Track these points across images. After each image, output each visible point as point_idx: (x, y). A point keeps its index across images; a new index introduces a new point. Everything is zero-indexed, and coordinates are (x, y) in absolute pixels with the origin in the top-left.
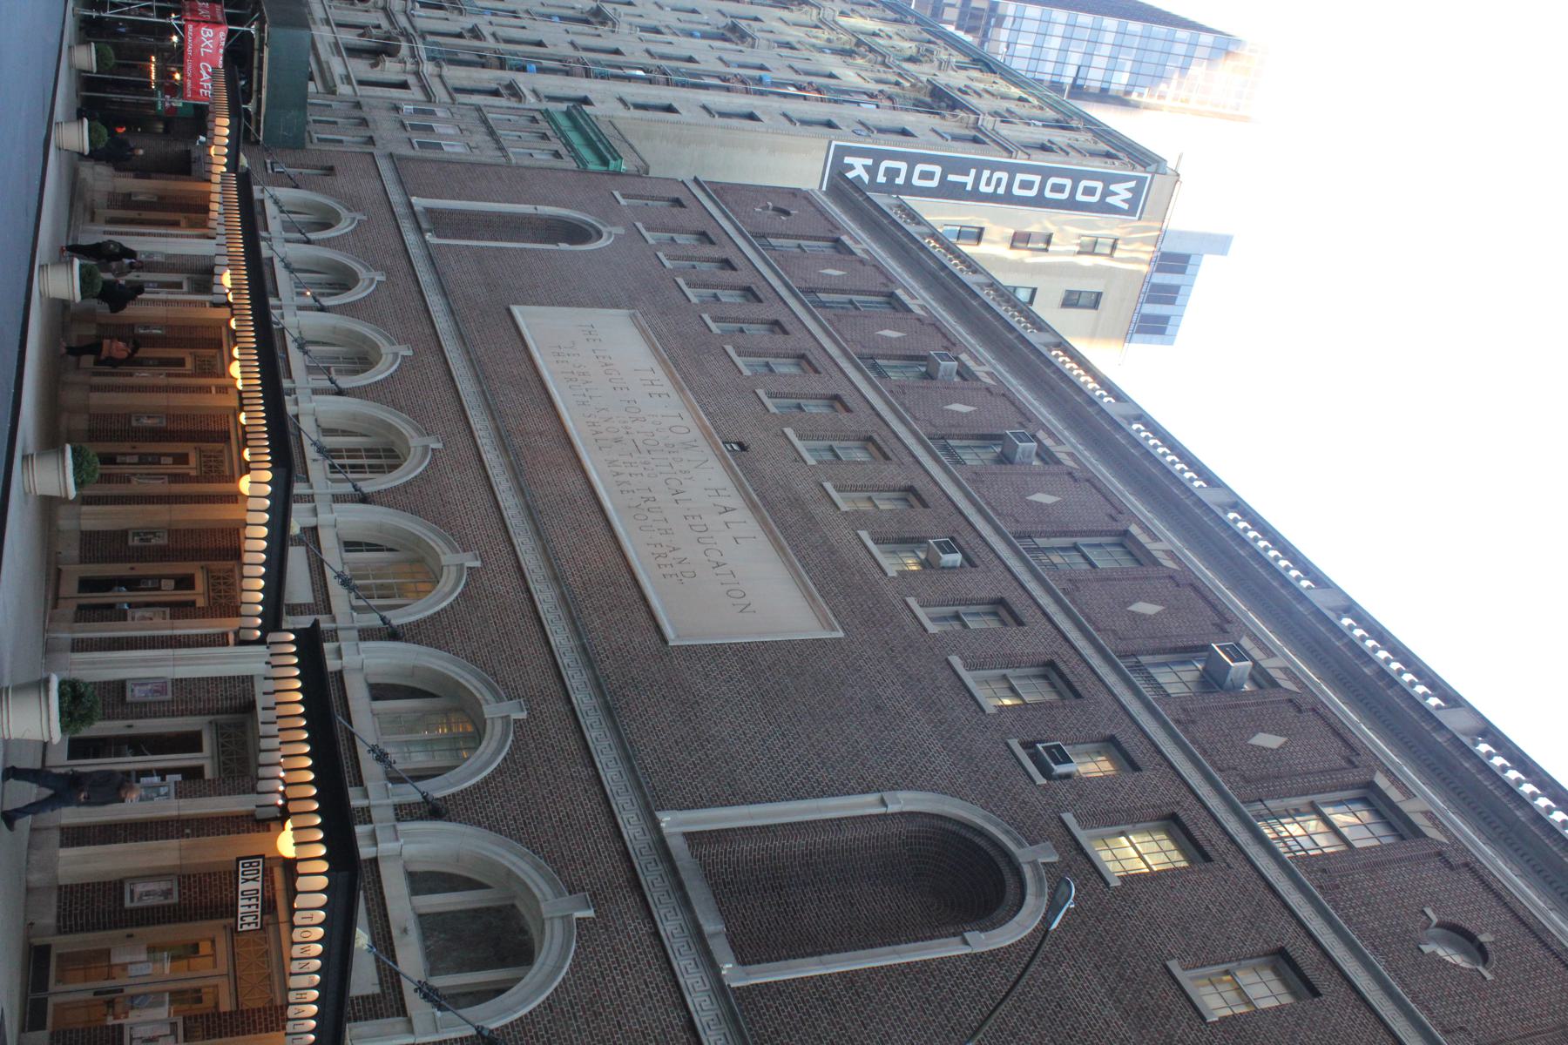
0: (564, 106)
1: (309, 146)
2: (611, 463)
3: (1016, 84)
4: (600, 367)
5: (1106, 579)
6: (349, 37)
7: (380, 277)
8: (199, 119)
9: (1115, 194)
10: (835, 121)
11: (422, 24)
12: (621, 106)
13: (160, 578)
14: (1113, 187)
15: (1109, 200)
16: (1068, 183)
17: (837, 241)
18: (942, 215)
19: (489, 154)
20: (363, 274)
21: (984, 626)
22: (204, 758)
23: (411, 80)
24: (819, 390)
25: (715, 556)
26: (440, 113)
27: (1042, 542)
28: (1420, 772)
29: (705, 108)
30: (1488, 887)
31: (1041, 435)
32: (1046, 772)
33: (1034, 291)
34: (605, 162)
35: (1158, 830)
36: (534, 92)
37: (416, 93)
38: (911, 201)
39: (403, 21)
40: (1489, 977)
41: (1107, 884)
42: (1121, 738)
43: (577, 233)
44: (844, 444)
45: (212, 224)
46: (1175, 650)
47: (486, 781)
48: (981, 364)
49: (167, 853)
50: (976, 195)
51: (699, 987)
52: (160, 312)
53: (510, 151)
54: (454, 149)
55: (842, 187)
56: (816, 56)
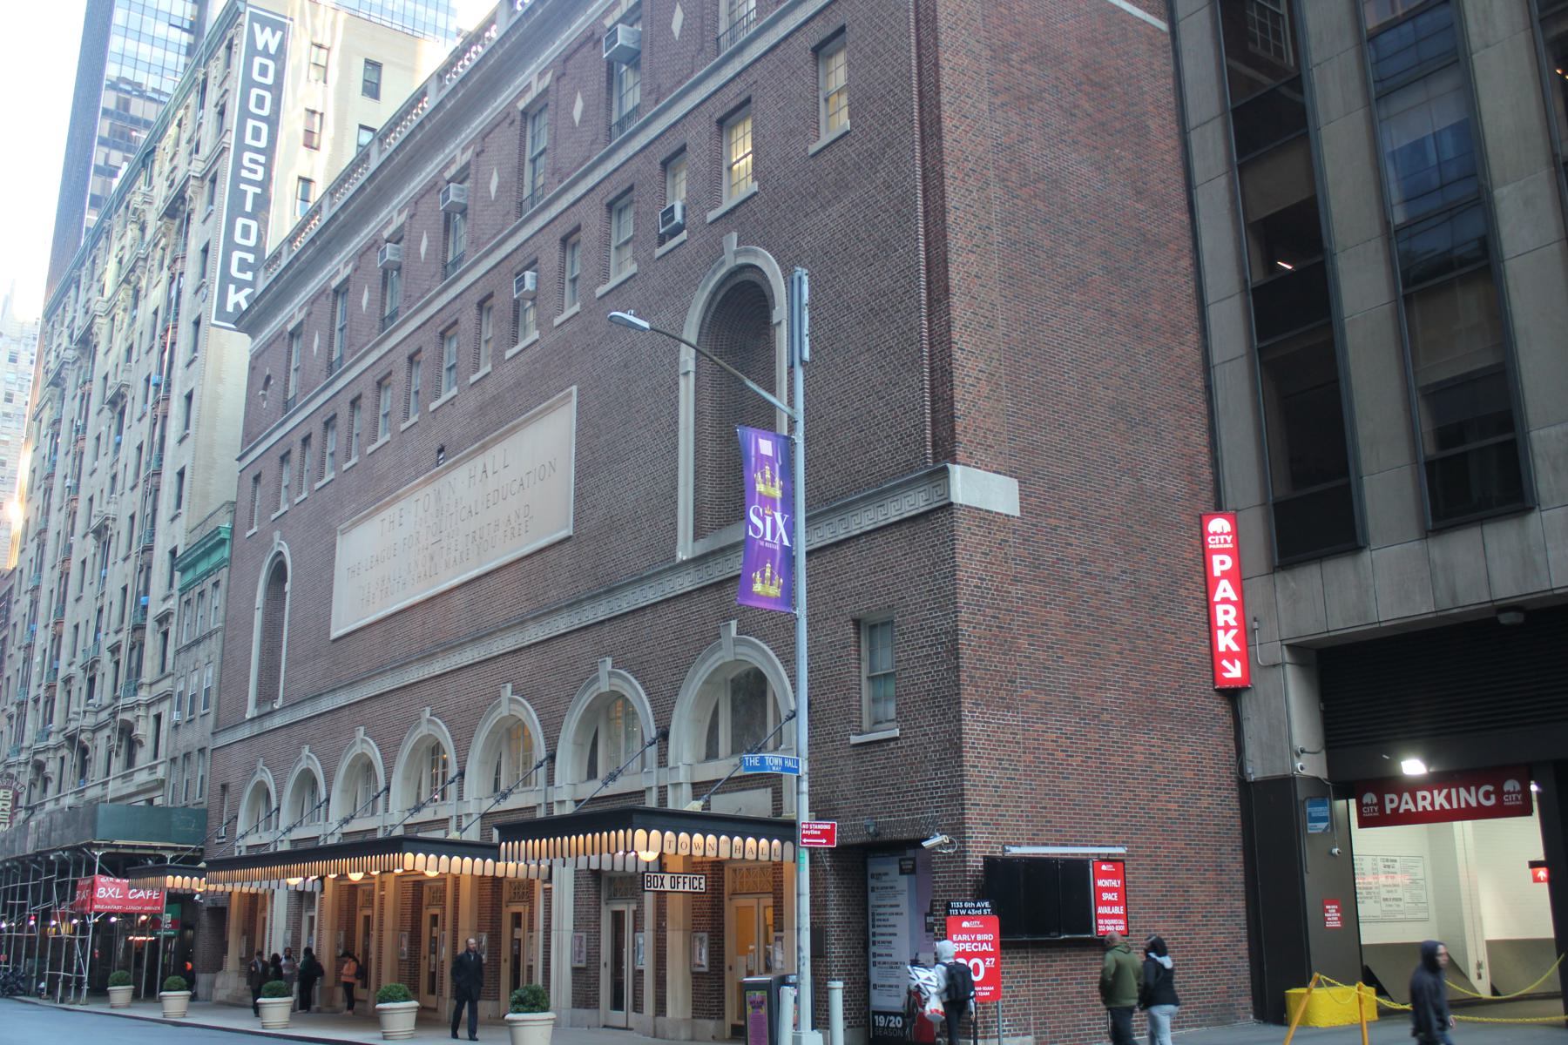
0: (177, 574)
1: (205, 805)
2: (447, 566)
3: (165, 130)
4: (384, 563)
5: (554, 140)
6: (117, 765)
7: (306, 750)
8: (180, 900)
9: (266, 45)
10: (194, 318)
11: (107, 700)
12: (177, 521)
13: (513, 939)
14: (260, 47)
15: (272, 50)
16: (255, 92)
17: (292, 334)
19: (214, 645)
20: (303, 765)
21: (684, 185)
22: (628, 909)
23: (153, 711)
25: (516, 486)
26: (180, 687)
27: (527, 192)
29: (181, 441)
32: (678, 229)
33: (361, 127)
34: (222, 542)
35: (730, 136)
36: (164, 600)
37: (164, 708)
39: (104, 716)
41: (755, 194)
42: (663, 156)
43: (278, 572)
45: (261, 891)
49: (675, 940)
50: (265, 184)
51: (871, 514)
52: (326, 934)
53: (213, 627)
54: (209, 676)
55: (248, 321)
56: (138, 324)
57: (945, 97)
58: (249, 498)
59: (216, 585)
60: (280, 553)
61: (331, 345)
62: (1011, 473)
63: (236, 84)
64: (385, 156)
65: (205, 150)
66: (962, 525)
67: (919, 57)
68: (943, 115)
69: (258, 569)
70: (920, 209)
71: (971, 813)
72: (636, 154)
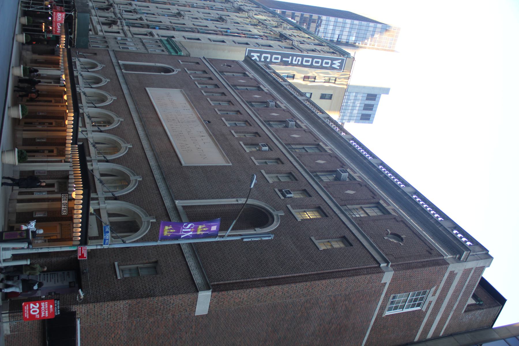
3: (307, 34)
4: (172, 105)
5: (310, 155)
6: (103, 20)
7: (108, 80)
8: (57, 40)
9: (335, 64)
10: (249, 43)
11: (124, 16)
13: (44, 150)
14: (334, 62)
15: (333, 66)
17: (245, 73)
19: (143, 50)
21: (299, 197)
22: (55, 189)
23: (121, 31)
26: (129, 40)
27: (293, 146)
28: (393, 201)
29: (209, 39)
30: (407, 226)
32: (284, 196)
33: (311, 94)
34: (177, 53)
35: (315, 211)
36: (158, 35)
37: (122, 35)
41: (297, 220)
42: (307, 190)
45: (60, 66)
46: (327, 171)
47: (130, 193)
49: (45, 205)
50: (292, 64)
51: (193, 265)
52: (45, 88)
54: (132, 48)
55: (248, 60)
56: (246, 26)
57: (332, 280)
58: (192, 61)
59: (163, 51)
60: (173, 71)
62: (210, 311)
63: (322, 55)
64: (303, 101)
65: (301, 46)
66: (191, 296)
67: (344, 271)
68: (326, 280)
69: (168, 64)
70: (295, 275)
71: (91, 306)
72: (307, 181)
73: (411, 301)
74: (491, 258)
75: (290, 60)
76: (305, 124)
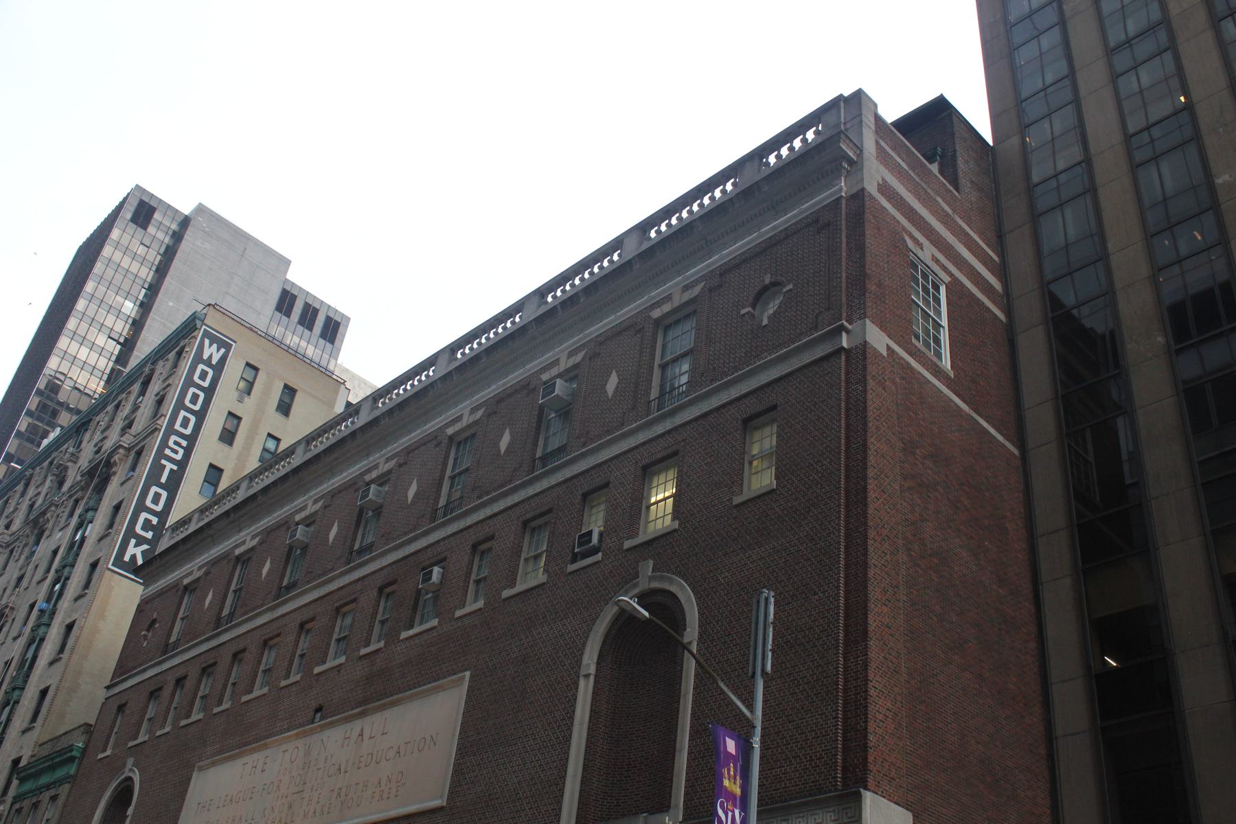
2: (305, 816)
3: (105, 407)
9: (211, 356)
12: (29, 734)
14: (205, 357)
15: (214, 362)
18: (190, 498)
24: (292, 638)
25: (392, 753)
28: (657, 286)
29: (51, 663)
30: (738, 266)
31: (367, 478)
32: (594, 551)
33: (270, 435)
34: (72, 759)
35: (651, 482)
38: (172, 519)
40: (790, 286)
41: (675, 531)
42: (586, 488)
43: (123, 795)
44: (337, 629)
48: (306, 506)
50: (183, 464)
57: (871, 473)
59: (54, 798)
60: (130, 779)
61: (223, 602)
64: (309, 455)
65: (138, 427)
67: (847, 437)
68: (869, 487)
73: (927, 303)
74: (859, 96)
75: (169, 466)
76: (382, 460)
